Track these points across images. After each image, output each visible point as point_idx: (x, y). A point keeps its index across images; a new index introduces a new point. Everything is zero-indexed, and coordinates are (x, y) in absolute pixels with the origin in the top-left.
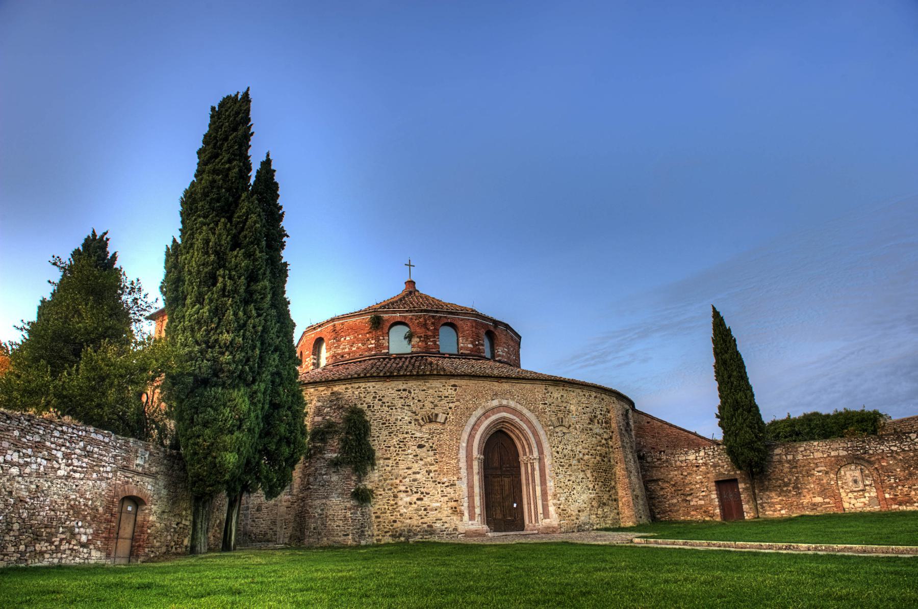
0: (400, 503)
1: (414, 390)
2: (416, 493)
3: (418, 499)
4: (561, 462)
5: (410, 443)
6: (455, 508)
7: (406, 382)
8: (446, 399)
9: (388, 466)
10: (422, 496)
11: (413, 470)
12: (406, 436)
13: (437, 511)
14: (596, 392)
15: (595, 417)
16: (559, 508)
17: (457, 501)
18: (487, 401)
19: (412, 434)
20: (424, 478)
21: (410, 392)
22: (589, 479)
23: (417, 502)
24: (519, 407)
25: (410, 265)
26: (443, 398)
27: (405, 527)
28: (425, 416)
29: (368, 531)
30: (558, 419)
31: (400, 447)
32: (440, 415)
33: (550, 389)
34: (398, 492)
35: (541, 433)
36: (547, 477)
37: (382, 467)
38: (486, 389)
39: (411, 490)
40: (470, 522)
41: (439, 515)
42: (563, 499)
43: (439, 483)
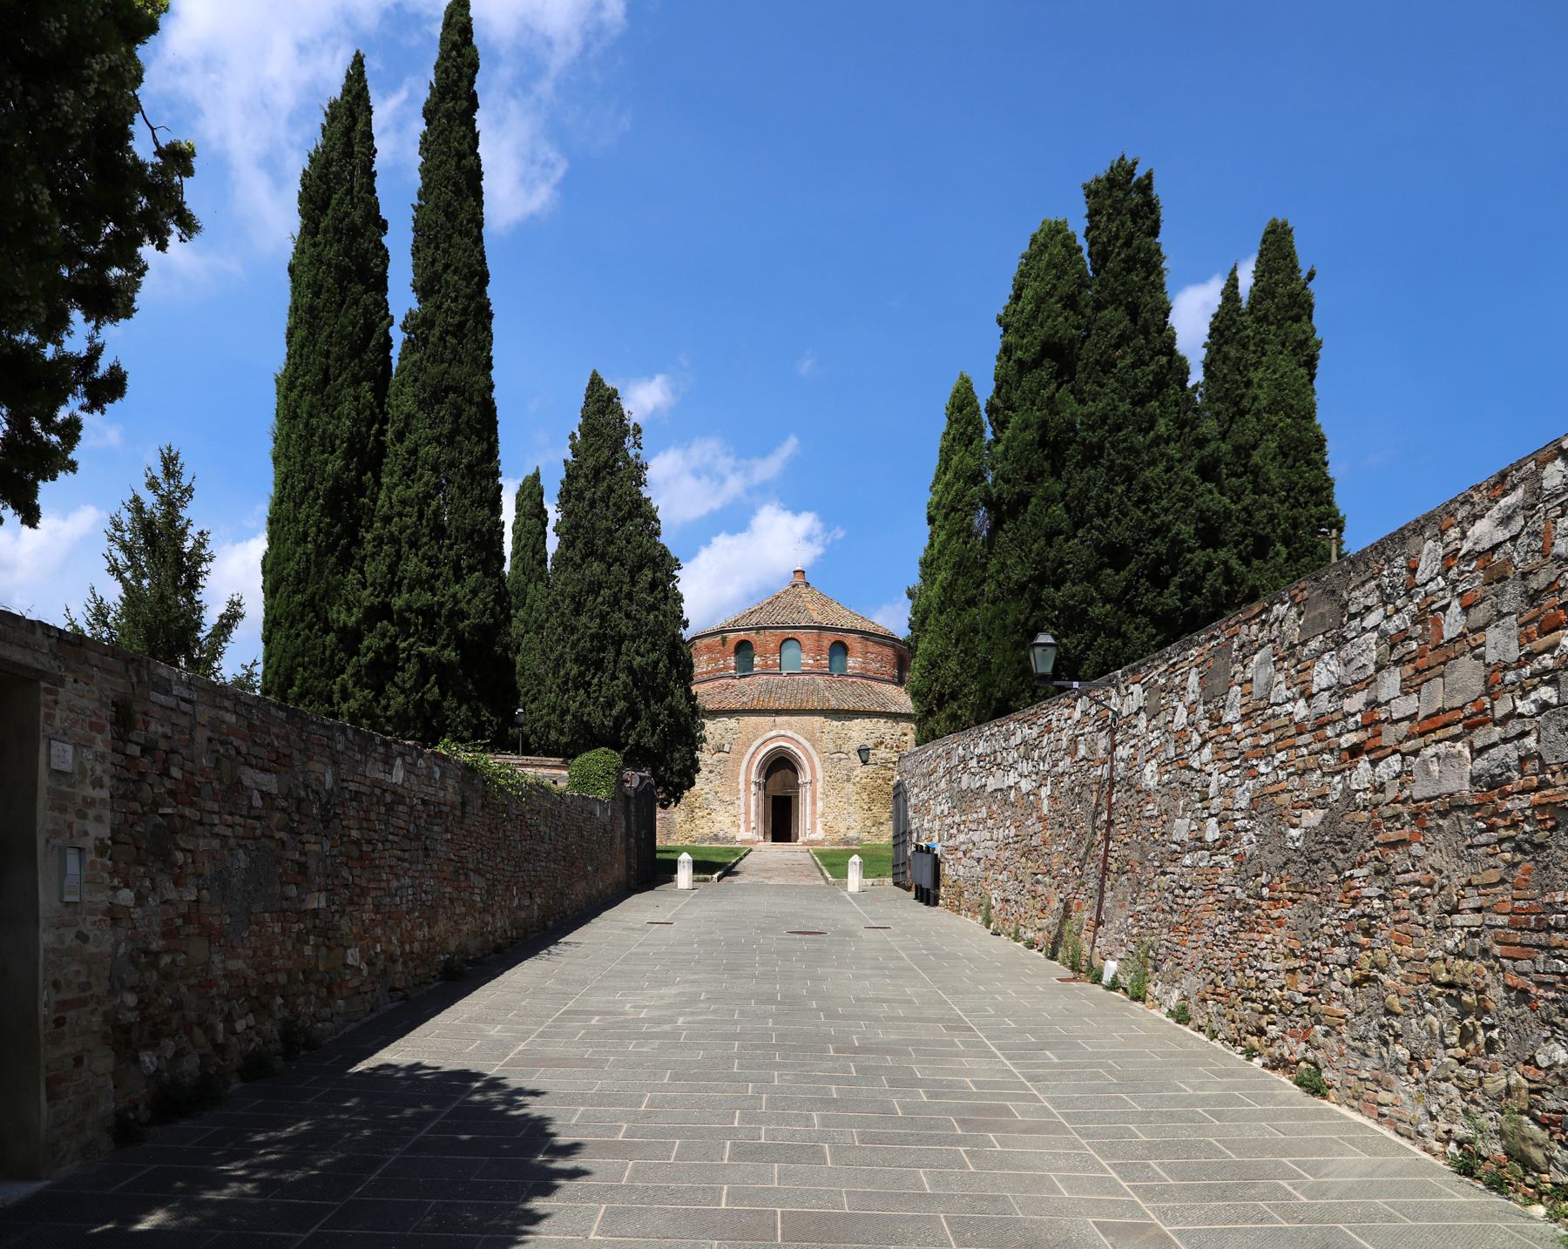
15: (882, 743)
18: (766, 731)
24: (796, 736)
42: (830, 818)
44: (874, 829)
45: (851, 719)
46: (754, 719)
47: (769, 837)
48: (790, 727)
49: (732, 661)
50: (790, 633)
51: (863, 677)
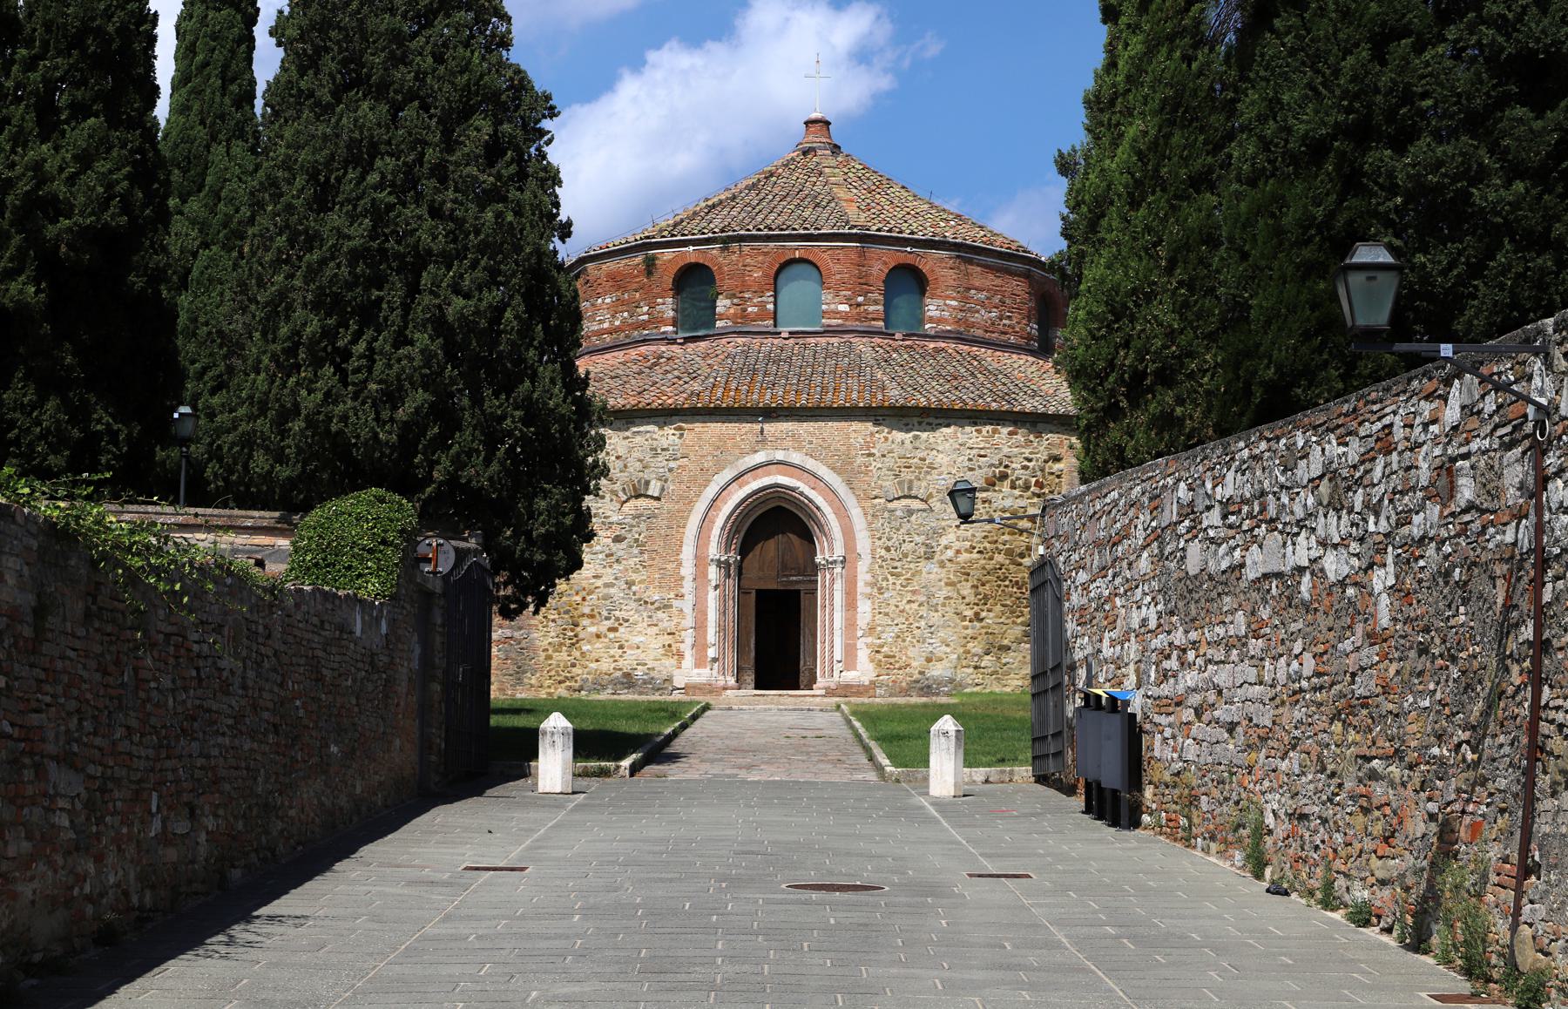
2: (607, 619)
3: (612, 629)
6: (670, 646)
11: (605, 579)
16: (878, 652)
18: (743, 454)
22: (967, 601)
24: (810, 464)
30: (900, 483)
32: (653, 483)
35: (856, 513)
36: (859, 597)
40: (696, 671)
41: (643, 656)
42: (888, 636)
44: (987, 661)
45: (933, 427)
46: (715, 429)
47: (750, 678)
49: (667, 307)
50: (797, 249)
51: (960, 338)
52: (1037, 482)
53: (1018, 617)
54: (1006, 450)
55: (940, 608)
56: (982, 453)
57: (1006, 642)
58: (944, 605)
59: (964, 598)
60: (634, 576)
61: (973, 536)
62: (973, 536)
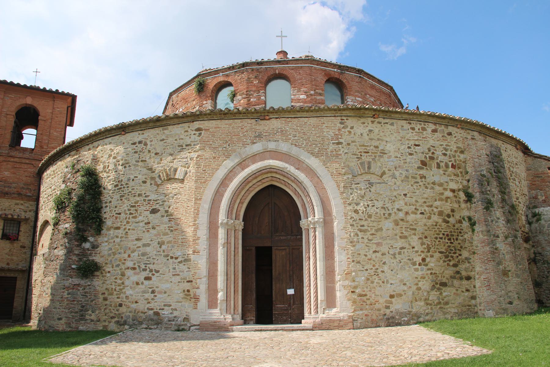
0: (127, 283)
1: (151, 141)
2: (145, 270)
4: (363, 226)
5: (143, 208)
6: (188, 291)
7: (142, 132)
8: (187, 148)
9: (117, 237)
10: (150, 275)
11: (144, 241)
12: (138, 199)
13: (167, 295)
14: (435, 124)
15: (432, 158)
17: (192, 281)
18: (245, 145)
19: (146, 196)
20: (155, 252)
21: (146, 144)
22: (416, 249)
23: (145, 282)
24: (295, 151)
25: (282, 36)
26: (184, 147)
27: (130, 312)
28: (162, 173)
29: (91, 315)
30: (362, 164)
31: (131, 214)
32: (179, 169)
33: (350, 122)
34: (126, 269)
37: (112, 238)
38: (245, 129)
39: (139, 266)
41: (168, 300)
43: (172, 258)
47: (252, 316)
48: (282, 132)
52: (452, 164)
53: (450, 261)
54: (432, 142)
55: (397, 256)
56: (417, 143)
57: (444, 280)
58: (400, 253)
59: (413, 248)
60: (165, 238)
61: (417, 201)
62: (417, 201)
